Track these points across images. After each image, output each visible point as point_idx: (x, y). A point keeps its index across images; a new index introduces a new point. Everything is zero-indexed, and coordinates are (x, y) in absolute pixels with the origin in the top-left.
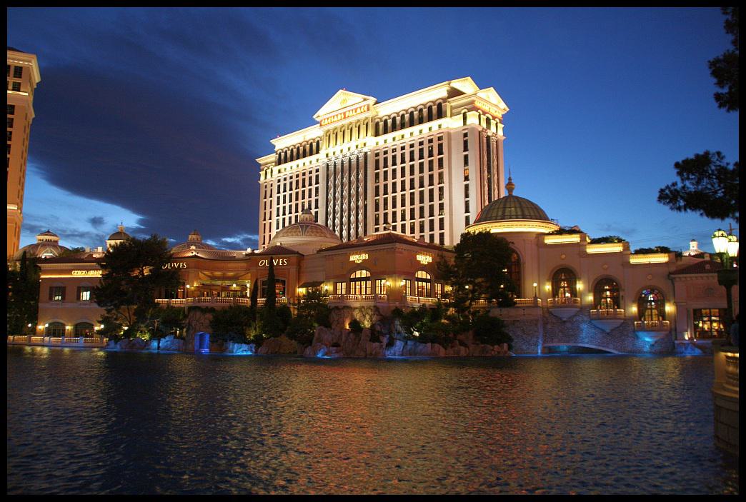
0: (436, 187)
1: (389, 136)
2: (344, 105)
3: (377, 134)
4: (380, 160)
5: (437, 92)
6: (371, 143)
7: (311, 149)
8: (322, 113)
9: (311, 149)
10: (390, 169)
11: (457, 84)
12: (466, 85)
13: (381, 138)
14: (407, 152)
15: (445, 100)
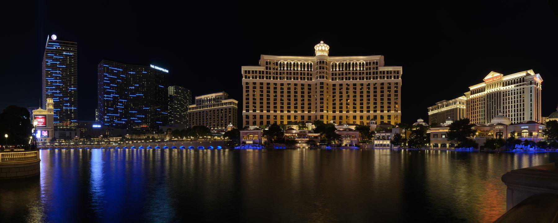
0: (522, 103)
1: (507, 87)
2: (492, 76)
3: (503, 86)
4: (505, 93)
5: (523, 74)
6: (502, 88)
7: (483, 90)
8: (486, 78)
9: (483, 90)
10: (508, 97)
11: (529, 72)
12: (531, 72)
13: (505, 88)
14: (513, 92)
15: (525, 76)
